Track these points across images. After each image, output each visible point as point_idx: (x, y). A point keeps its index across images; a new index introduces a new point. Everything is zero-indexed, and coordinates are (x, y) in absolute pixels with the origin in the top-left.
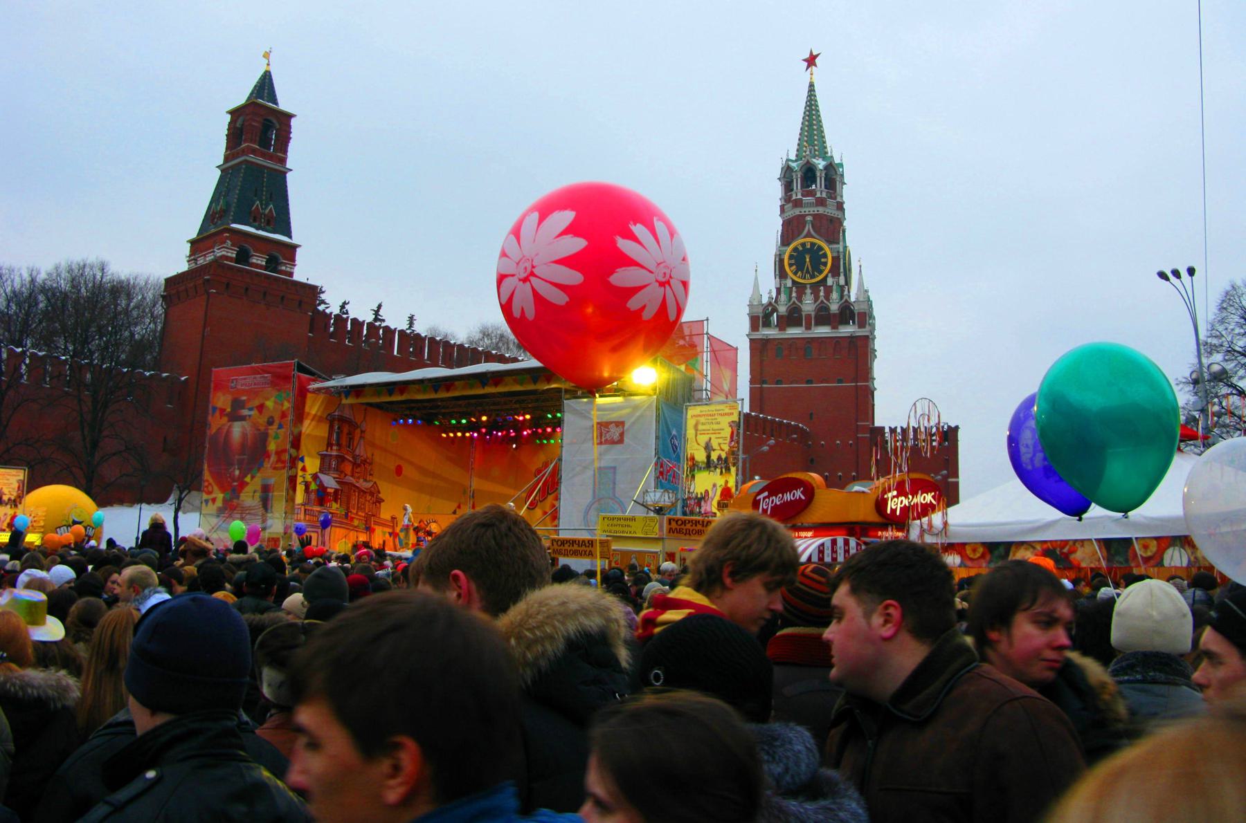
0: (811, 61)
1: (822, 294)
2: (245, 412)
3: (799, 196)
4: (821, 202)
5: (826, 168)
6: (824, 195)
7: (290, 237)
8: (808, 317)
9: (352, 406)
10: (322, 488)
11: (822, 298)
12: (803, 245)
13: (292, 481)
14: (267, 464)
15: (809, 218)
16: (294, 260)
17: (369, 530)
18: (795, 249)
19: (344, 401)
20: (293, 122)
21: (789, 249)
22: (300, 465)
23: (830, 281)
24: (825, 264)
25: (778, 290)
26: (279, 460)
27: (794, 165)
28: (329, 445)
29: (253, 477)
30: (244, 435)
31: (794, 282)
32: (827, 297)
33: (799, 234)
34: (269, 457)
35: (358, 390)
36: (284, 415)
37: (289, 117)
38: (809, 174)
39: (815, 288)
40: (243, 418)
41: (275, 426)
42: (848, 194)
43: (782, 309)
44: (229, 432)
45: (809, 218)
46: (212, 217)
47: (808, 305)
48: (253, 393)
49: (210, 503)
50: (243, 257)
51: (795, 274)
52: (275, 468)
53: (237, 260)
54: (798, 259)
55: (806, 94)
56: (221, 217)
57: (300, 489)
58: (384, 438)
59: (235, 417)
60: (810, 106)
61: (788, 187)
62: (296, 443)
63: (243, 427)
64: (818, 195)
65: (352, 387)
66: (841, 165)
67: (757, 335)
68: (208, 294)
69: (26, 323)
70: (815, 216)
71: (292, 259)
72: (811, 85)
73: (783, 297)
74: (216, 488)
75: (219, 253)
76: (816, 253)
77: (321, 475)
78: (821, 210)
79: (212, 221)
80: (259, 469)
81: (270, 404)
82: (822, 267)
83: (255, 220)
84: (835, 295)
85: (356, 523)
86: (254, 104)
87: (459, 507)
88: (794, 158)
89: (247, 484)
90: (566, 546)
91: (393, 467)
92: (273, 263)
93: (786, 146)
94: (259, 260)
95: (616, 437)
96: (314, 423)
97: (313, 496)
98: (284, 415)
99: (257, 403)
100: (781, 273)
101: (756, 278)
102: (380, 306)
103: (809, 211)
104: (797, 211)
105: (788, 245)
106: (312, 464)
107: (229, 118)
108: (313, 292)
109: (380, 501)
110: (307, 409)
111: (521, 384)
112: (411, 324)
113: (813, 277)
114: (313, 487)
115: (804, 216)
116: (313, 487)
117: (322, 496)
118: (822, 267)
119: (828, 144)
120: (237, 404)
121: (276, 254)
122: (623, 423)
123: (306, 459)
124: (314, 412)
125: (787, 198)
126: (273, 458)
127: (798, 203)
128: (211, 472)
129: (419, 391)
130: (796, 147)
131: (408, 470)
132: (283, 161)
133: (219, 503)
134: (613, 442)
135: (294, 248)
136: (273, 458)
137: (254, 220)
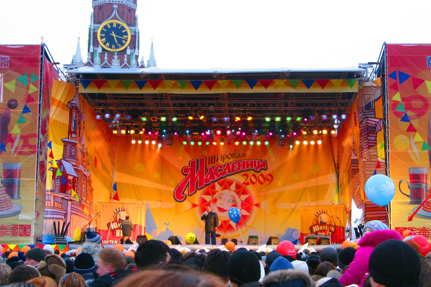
1: (126, 59)
10: (65, 175)
12: (111, 24)
13: (42, 166)
14: (10, 149)
15: (115, 6)
18: (106, 27)
21: (102, 26)
23: (129, 52)
26: (26, 145)
28: (70, 133)
31: (103, 49)
33: (108, 17)
36: (30, 99)
45: (115, 6)
51: (105, 44)
52: (20, 153)
54: (107, 33)
57: (49, 174)
77: (63, 162)
97: (58, 183)
98: (30, 99)
101: (79, 44)
105: (100, 23)
106: (57, 150)
110: (53, 95)
111: (294, 87)
113: (117, 47)
117: (65, 184)
123: (53, 145)
124: (58, 98)
126: (18, 143)
129: (175, 86)
136: (18, 143)
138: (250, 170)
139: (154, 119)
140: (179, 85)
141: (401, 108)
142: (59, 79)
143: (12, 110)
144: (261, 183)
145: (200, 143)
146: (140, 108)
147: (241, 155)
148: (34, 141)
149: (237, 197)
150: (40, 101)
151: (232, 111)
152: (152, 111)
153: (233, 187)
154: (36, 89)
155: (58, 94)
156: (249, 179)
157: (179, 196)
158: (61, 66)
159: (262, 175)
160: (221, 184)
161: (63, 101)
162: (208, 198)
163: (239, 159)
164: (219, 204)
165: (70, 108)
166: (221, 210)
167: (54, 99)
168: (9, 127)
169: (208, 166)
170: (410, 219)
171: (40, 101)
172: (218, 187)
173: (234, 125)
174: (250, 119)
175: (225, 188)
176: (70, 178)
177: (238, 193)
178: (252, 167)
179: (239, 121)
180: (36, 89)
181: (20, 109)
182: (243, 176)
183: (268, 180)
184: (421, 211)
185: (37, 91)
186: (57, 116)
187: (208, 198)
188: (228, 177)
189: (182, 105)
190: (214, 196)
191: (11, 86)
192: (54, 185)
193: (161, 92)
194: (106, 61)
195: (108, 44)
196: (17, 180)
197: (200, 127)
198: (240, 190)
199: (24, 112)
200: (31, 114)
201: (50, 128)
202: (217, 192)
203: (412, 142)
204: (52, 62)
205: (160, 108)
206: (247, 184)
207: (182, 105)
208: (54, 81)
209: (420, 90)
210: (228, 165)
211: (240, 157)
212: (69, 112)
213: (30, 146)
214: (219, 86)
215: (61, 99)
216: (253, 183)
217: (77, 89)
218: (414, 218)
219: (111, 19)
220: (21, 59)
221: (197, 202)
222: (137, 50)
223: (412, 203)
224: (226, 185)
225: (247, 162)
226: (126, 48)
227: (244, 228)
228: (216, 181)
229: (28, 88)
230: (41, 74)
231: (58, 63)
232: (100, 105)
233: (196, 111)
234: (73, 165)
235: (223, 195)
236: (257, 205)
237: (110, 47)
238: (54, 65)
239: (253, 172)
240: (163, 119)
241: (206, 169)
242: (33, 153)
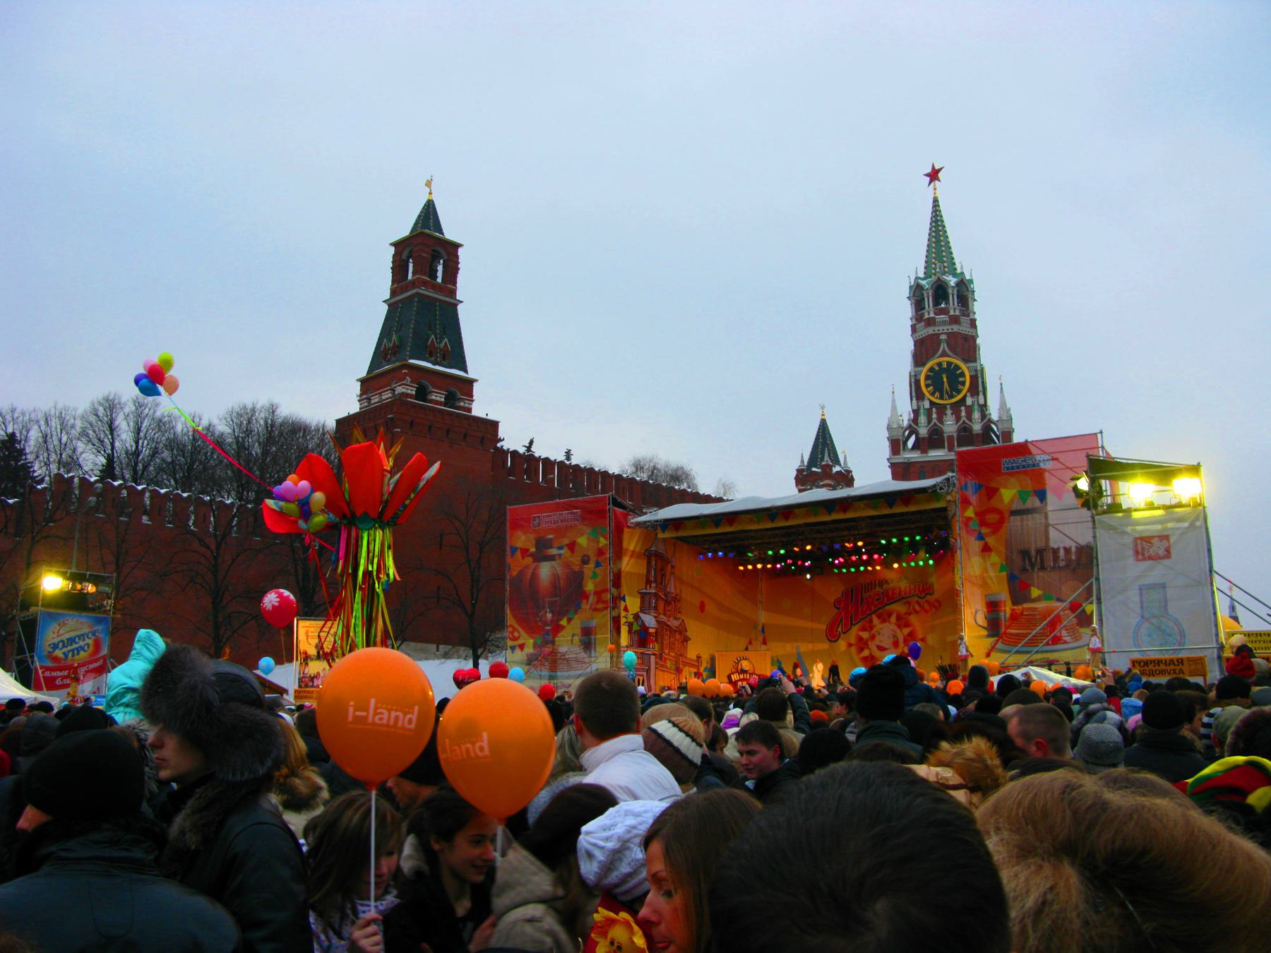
0: (934, 175)
1: (963, 414)
2: (554, 551)
3: (932, 315)
4: (955, 320)
5: (958, 284)
6: (958, 313)
7: (466, 372)
8: (950, 438)
9: (664, 540)
10: (644, 628)
11: (964, 419)
12: (939, 364)
13: (616, 622)
14: (585, 606)
15: (943, 337)
17: (679, 671)
18: (931, 369)
19: (661, 535)
20: (461, 251)
21: (925, 370)
23: (969, 401)
24: (963, 383)
25: (916, 412)
26: (599, 601)
27: (923, 282)
28: (648, 582)
29: (569, 620)
30: (555, 577)
31: (931, 403)
32: (969, 416)
33: (934, 354)
35: (677, 523)
36: (601, 552)
37: (456, 246)
38: (940, 291)
39: (956, 407)
40: (551, 558)
41: (591, 565)
42: (981, 309)
43: (923, 431)
44: (535, 576)
45: (943, 337)
46: (381, 354)
47: (950, 426)
48: (560, 532)
50: (422, 393)
51: (933, 394)
52: (596, 610)
53: (417, 397)
54: (935, 379)
55: (930, 210)
56: (394, 354)
57: (624, 629)
58: (691, 571)
59: (540, 556)
60: (936, 221)
61: (918, 305)
62: (617, 582)
63: (553, 567)
64: (952, 313)
65: (666, 521)
66: (971, 281)
67: (898, 459)
69: (190, 469)
70: (949, 335)
71: (469, 394)
72: (936, 201)
73: (923, 419)
75: (400, 390)
76: (954, 375)
78: (955, 328)
79: (385, 358)
80: (576, 612)
81: (583, 541)
82: (960, 387)
83: (431, 355)
84: (976, 415)
85: (668, 664)
86: (422, 233)
87: (750, 643)
88: (922, 275)
89: (563, 628)
90: (1151, 667)
91: (698, 604)
92: (451, 399)
93: (914, 264)
94: (438, 396)
95: (1162, 552)
96: (633, 560)
97: (636, 638)
98: (601, 552)
99: (566, 541)
100: (917, 394)
101: (894, 401)
102: (531, 442)
103: (943, 329)
104: (930, 330)
105: (924, 365)
106: (633, 604)
107: (393, 249)
108: (491, 427)
109: (686, 640)
110: (625, 545)
111: (875, 508)
112: (568, 458)
113: (951, 397)
114: (636, 627)
115: (938, 335)
118: (960, 387)
119: (956, 261)
120: (543, 544)
121: (452, 389)
122: (1167, 537)
124: (631, 548)
125: (919, 316)
126: (592, 599)
127: (930, 322)
128: (515, 617)
129: (751, 521)
130: (923, 264)
131: (710, 607)
132: (453, 293)
133: (529, 649)
134: (1156, 558)
135: (471, 382)
136: (592, 599)
137: (430, 355)
141: (974, 525)
144: (927, 612)
149: (898, 631)
153: (893, 619)
157: (832, 636)
160: (879, 617)
162: (865, 635)
164: (877, 642)
166: (881, 649)
170: (988, 655)
172: (876, 620)
175: (884, 621)
176: (651, 631)
177: (899, 626)
181: (591, 565)
184: (1000, 645)
187: (865, 635)
192: (631, 639)
194: (935, 421)
195: (937, 394)
198: (902, 622)
203: (988, 564)
206: (910, 614)
209: (994, 503)
216: (917, 612)
218: (992, 654)
219: (941, 356)
221: (853, 641)
222: (981, 397)
223: (989, 636)
224: (884, 618)
226: (965, 397)
229: (598, 542)
237: (941, 398)
242: (606, 608)
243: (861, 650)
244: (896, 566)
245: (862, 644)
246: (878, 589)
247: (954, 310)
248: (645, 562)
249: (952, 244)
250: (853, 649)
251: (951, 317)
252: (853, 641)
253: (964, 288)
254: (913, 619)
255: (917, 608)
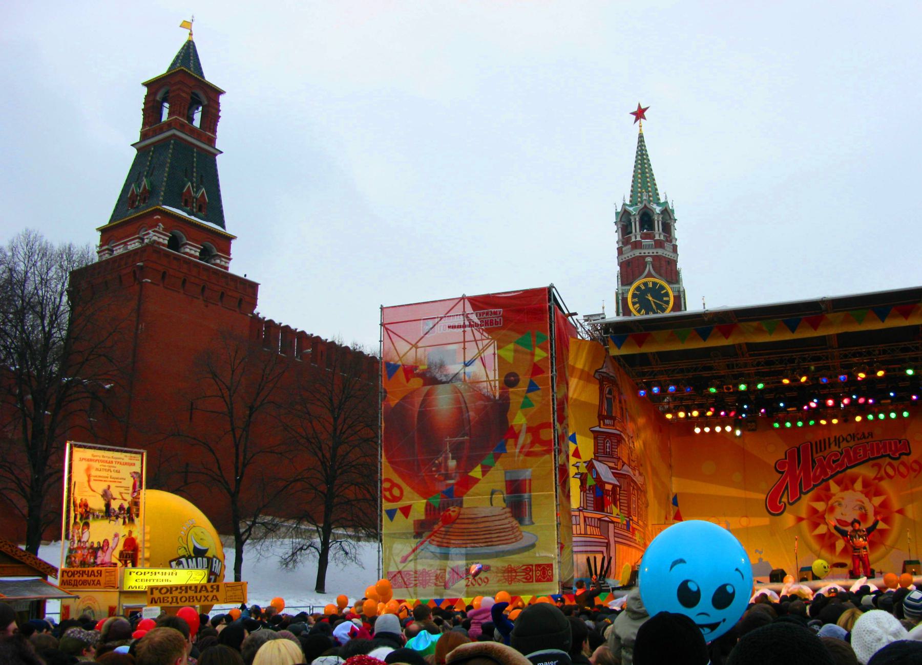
0: (640, 114)
3: (639, 239)
4: (659, 244)
6: (662, 238)
10: (600, 483)
12: (645, 284)
14: (512, 449)
15: (649, 259)
16: (229, 254)
18: (638, 288)
20: (222, 99)
22: (572, 447)
24: (667, 302)
26: (536, 440)
27: (631, 209)
28: (601, 417)
34: (516, 436)
36: (537, 370)
37: (219, 92)
41: (522, 387)
45: (649, 259)
49: (399, 515)
52: (528, 454)
56: (144, 200)
57: (574, 485)
64: (657, 237)
66: (673, 211)
68: (141, 283)
71: (227, 252)
72: (641, 137)
74: (407, 489)
76: (658, 292)
77: (596, 463)
78: (660, 252)
80: (496, 457)
83: (186, 205)
88: (628, 202)
89: (476, 480)
92: (206, 254)
93: (619, 192)
94: (192, 251)
97: (591, 496)
104: (637, 253)
105: (630, 284)
106: (586, 446)
108: (249, 290)
110: (571, 361)
114: (590, 482)
116: (590, 482)
117: (599, 497)
121: (208, 244)
123: (578, 437)
127: (637, 245)
129: (759, 330)
132: (212, 141)
135: (229, 239)
137: (185, 202)
138: (883, 456)
139: (728, 389)
140: (765, 328)
142: (579, 337)
143: (511, 390)
144: (903, 476)
145: (800, 424)
146: (705, 374)
147: (866, 435)
148: (547, 434)
149: (866, 500)
150: (552, 371)
151: (849, 366)
152: (723, 376)
153: (858, 485)
154: (544, 354)
155: (579, 360)
156: (883, 472)
157: (774, 507)
158: (580, 317)
159: (903, 463)
160: (838, 483)
161: (586, 369)
162: (820, 506)
163: (864, 440)
165: (599, 380)
167: (573, 368)
168: (509, 417)
169: (815, 456)
171: (552, 371)
172: (834, 488)
173: (853, 386)
174: (880, 373)
175: (846, 488)
177: (867, 495)
178: (885, 451)
179: (863, 379)
180: (544, 354)
181: (522, 387)
182: (873, 466)
183: (914, 470)
185: (547, 358)
186: (580, 391)
187: (820, 506)
188: (849, 471)
189: (769, 363)
190: (830, 503)
191: (508, 353)
192: (585, 500)
193: (737, 342)
196: (526, 495)
197: (799, 395)
198: (871, 489)
199: (529, 391)
200: (539, 392)
201: (570, 412)
202: (834, 495)
204: (566, 312)
205: (736, 371)
206: (881, 479)
207: (769, 363)
208: (571, 340)
210: (847, 452)
211: (864, 437)
212: (597, 387)
213: (543, 443)
214: (830, 324)
215: (584, 366)
216: (890, 477)
217: (607, 351)
220: (519, 311)
221: (804, 514)
224: (847, 484)
225: (878, 444)
227: (882, 550)
228: (832, 477)
229: (533, 354)
230: (551, 331)
231: (575, 314)
232: (644, 374)
233: (794, 370)
234: (611, 468)
235: (843, 498)
236: (900, 512)
238: (570, 318)
239: (888, 460)
240: (743, 387)
241: (813, 461)
242: (548, 452)
243: (815, 525)
244: (858, 419)
245: (816, 518)
246: (834, 448)
247: (659, 235)
248: (596, 387)
249: (655, 177)
250: (804, 525)
251: (656, 241)
252: (804, 514)
253: (667, 214)
254: (885, 484)
255: (890, 471)
